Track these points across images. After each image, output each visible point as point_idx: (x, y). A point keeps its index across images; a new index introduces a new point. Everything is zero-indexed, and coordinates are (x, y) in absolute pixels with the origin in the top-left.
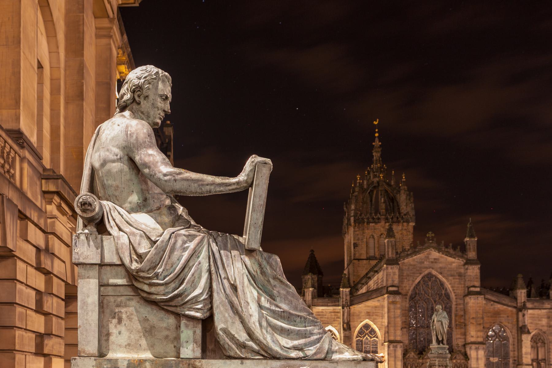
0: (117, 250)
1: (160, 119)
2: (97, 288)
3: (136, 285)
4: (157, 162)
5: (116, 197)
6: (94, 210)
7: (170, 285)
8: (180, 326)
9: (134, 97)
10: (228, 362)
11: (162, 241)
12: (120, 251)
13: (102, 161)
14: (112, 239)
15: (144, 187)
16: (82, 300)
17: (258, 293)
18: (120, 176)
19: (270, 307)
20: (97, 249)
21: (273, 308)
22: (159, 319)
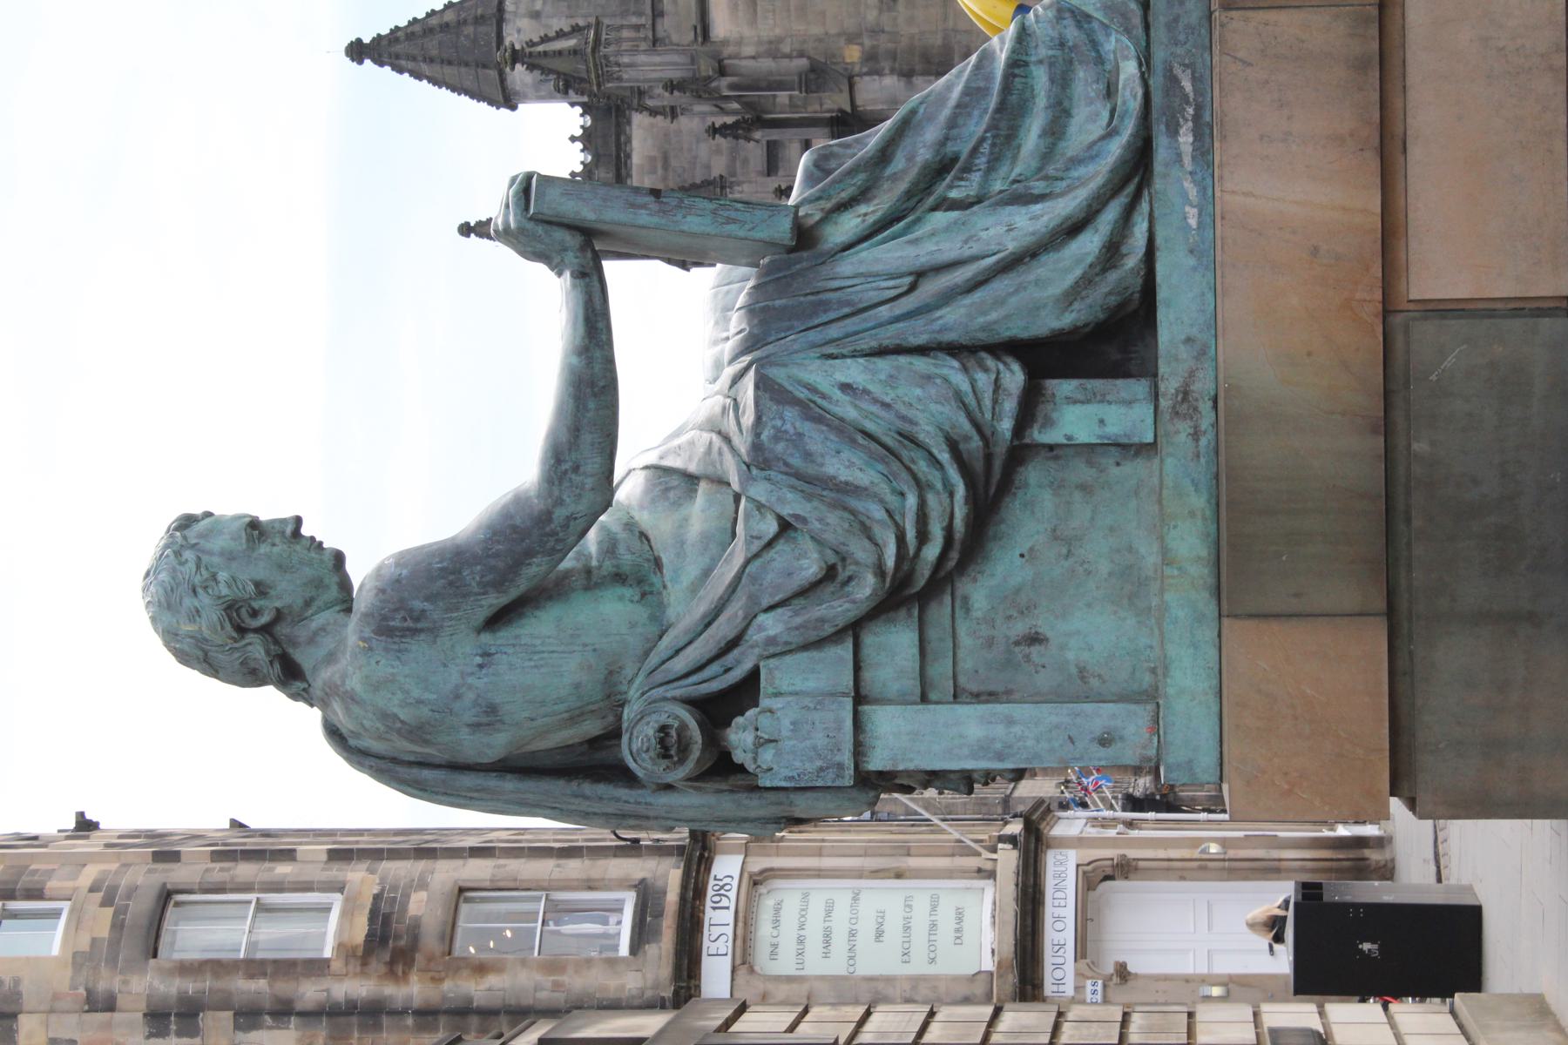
0: (806, 647)
2: (932, 707)
7: (920, 475)
8: (1051, 447)
9: (256, 630)
10: (1162, 294)
12: (813, 636)
14: (773, 662)
17: (934, 209)
18: (545, 655)
19: (980, 170)
21: (981, 161)
22: (1028, 512)
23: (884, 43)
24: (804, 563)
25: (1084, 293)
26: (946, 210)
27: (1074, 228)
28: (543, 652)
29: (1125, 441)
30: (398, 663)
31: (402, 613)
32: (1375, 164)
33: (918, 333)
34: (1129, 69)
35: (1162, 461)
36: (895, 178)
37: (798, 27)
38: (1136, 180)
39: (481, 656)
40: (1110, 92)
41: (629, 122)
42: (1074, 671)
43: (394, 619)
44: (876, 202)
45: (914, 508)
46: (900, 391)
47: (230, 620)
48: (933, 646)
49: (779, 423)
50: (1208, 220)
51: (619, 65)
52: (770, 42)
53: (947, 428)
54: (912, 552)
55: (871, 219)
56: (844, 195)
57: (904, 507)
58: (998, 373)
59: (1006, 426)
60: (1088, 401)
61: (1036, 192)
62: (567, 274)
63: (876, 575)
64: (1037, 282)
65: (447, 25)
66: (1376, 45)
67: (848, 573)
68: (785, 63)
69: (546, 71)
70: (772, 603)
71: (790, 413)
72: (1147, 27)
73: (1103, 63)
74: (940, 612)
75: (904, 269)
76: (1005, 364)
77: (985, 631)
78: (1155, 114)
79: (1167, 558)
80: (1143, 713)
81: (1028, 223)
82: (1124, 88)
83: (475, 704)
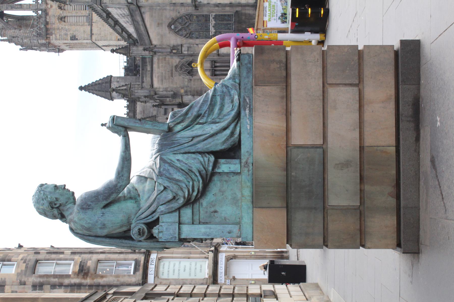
0: (169, 213)
2: (194, 225)
7: (193, 178)
8: (219, 173)
9: (56, 208)
10: (242, 142)
12: (170, 210)
16: (203, 235)
17: (197, 124)
18: (116, 214)
21: (206, 115)
23: (189, 89)
24: (169, 195)
25: (227, 142)
26: (199, 125)
27: (225, 129)
28: (115, 213)
29: (235, 172)
30: (85, 215)
31: (86, 205)
33: (193, 149)
34: (236, 97)
35: (242, 176)
36: (189, 118)
37: (171, 85)
38: (237, 119)
39: (102, 214)
40: (232, 102)
41: (136, 104)
42: (223, 218)
43: (84, 206)
44: (185, 123)
45: (192, 185)
46: (189, 161)
47: (50, 205)
48: (195, 213)
49: (164, 167)
50: (252, 128)
51: (134, 92)
52: (166, 88)
53: (198, 169)
54: (191, 193)
55: (184, 126)
56: (178, 121)
57: (189, 185)
58: (209, 158)
59: (210, 168)
60: (227, 164)
61: (217, 121)
62: (121, 136)
63: (183, 198)
64: (217, 139)
65: (100, 83)
66: (285, 94)
67: (178, 198)
68: (169, 93)
69: (120, 93)
70: (162, 204)
71: (166, 165)
72: (240, 89)
73: (231, 96)
74: (196, 206)
75: (190, 136)
76: (210, 156)
77: (205, 210)
78: (241, 107)
79: (243, 195)
80: (237, 227)
81: (215, 127)
82: (235, 101)
83: (101, 223)
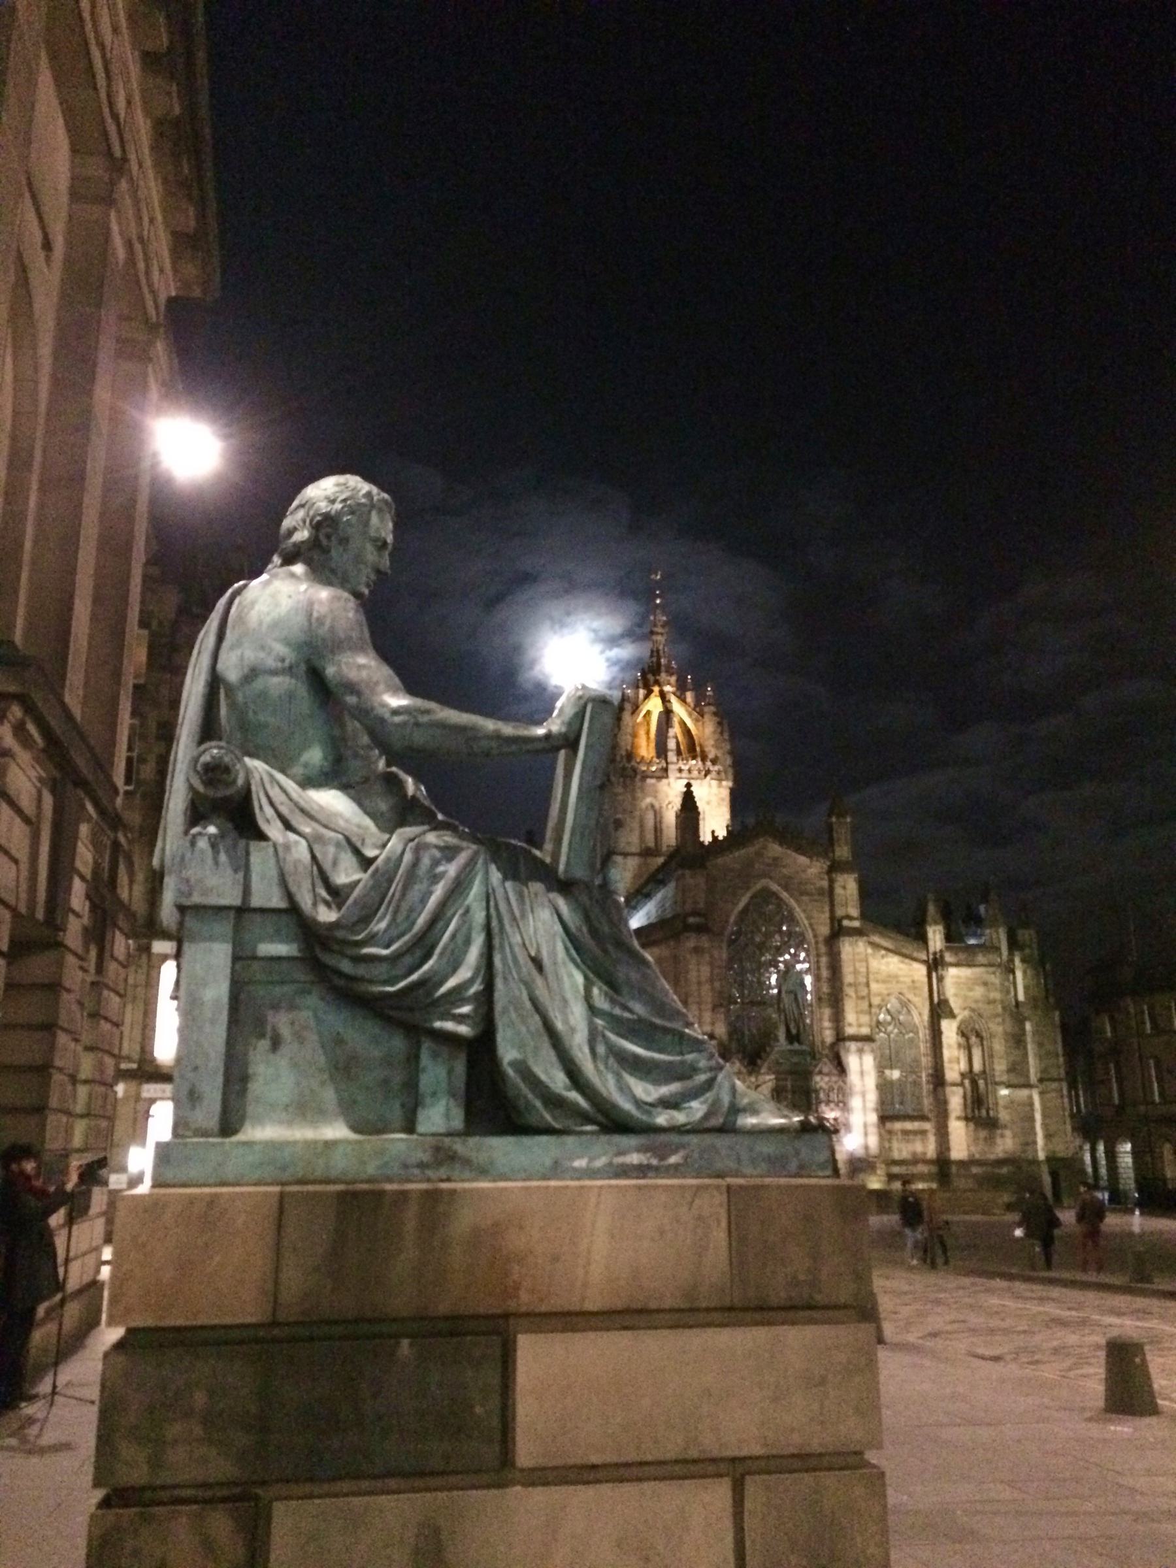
1: (368, 586)
3: (320, 955)
4: (377, 683)
5: (273, 750)
6: (234, 781)
8: (417, 1057)
10: (527, 1141)
11: (388, 859)
13: (246, 670)
14: (271, 850)
15: (337, 732)
17: (586, 978)
20: (236, 871)
21: (617, 1011)
32: (619, 1305)
80: (213, 1123)
81: (578, 1043)
